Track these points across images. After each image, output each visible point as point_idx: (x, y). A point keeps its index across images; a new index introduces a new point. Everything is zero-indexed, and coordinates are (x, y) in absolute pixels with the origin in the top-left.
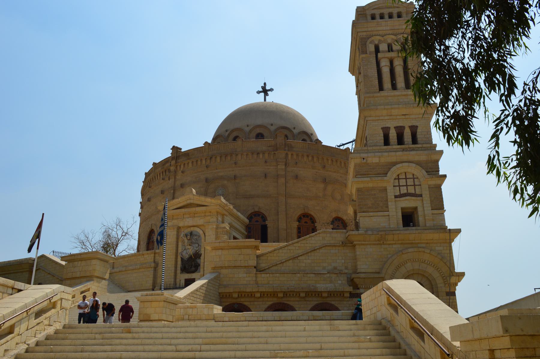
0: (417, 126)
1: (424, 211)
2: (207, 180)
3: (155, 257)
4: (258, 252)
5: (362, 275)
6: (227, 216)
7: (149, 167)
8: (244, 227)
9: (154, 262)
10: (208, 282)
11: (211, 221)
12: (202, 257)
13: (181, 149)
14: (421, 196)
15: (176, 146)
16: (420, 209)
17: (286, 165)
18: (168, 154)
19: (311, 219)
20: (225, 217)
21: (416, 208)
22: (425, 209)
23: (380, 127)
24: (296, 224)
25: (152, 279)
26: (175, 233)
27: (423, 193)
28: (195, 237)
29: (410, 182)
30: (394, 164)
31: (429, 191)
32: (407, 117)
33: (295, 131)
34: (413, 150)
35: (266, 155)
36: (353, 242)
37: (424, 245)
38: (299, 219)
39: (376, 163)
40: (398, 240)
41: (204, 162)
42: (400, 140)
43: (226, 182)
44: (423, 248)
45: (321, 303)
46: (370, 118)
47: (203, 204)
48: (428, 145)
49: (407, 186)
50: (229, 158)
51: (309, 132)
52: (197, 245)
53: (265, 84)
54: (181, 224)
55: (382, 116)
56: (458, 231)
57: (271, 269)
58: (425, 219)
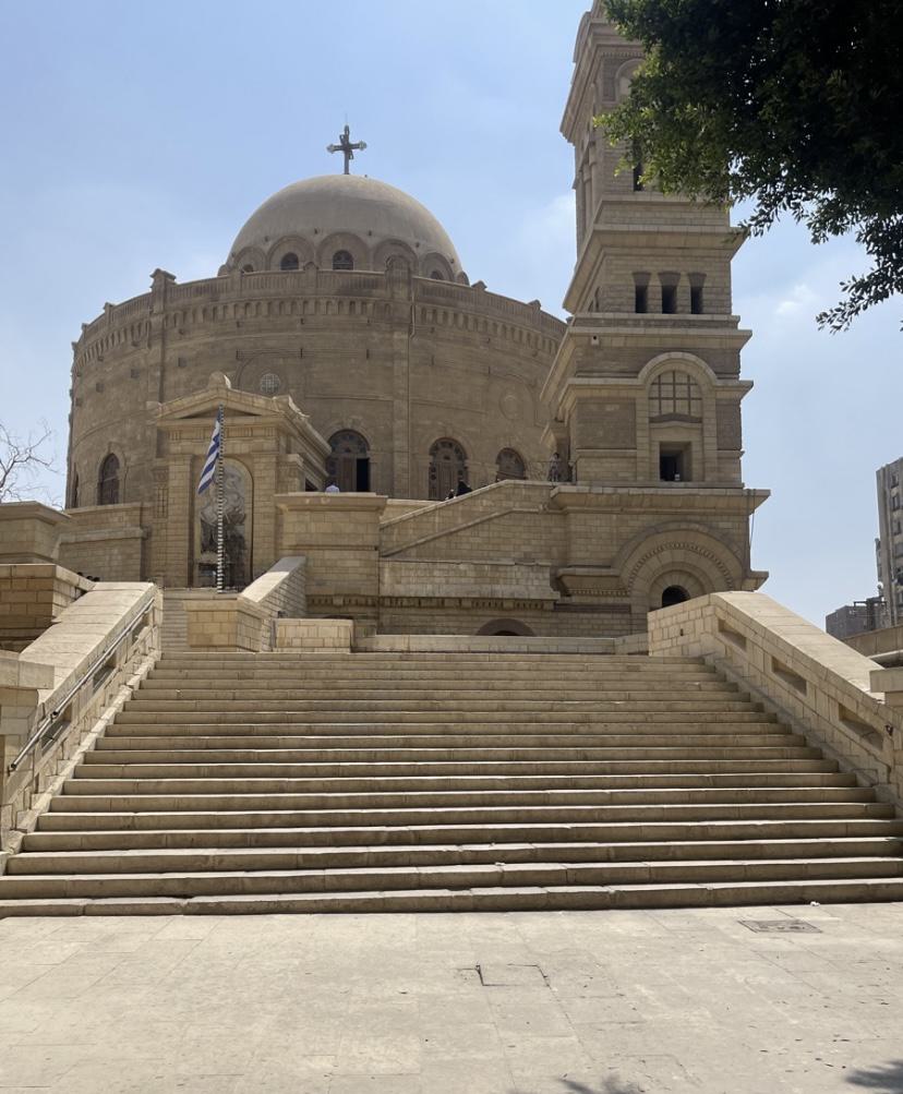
0: (705, 275)
1: (704, 448)
3: (141, 515)
4: (384, 520)
5: (580, 571)
6: (295, 438)
7: (94, 312)
10: (289, 578)
11: (240, 438)
12: (247, 522)
13: (174, 278)
14: (700, 420)
15: (163, 269)
16: (695, 448)
18: (144, 286)
19: (457, 451)
21: (688, 445)
22: (706, 447)
23: (630, 272)
24: (427, 460)
25: (139, 562)
26: (188, 468)
27: (706, 414)
28: (232, 480)
29: (681, 391)
30: (654, 352)
31: (717, 412)
32: (686, 252)
33: (420, 252)
34: (691, 324)
36: (566, 505)
37: (698, 518)
38: (434, 450)
39: (619, 348)
40: (651, 506)
41: (231, 311)
42: (668, 305)
44: (697, 522)
45: (498, 621)
46: (613, 250)
47: (248, 410)
48: (724, 318)
49: (674, 398)
51: (448, 256)
52: (236, 497)
53: (347, 129)
55: (637, 247)
56: (764, 495)
58: (704, 469)
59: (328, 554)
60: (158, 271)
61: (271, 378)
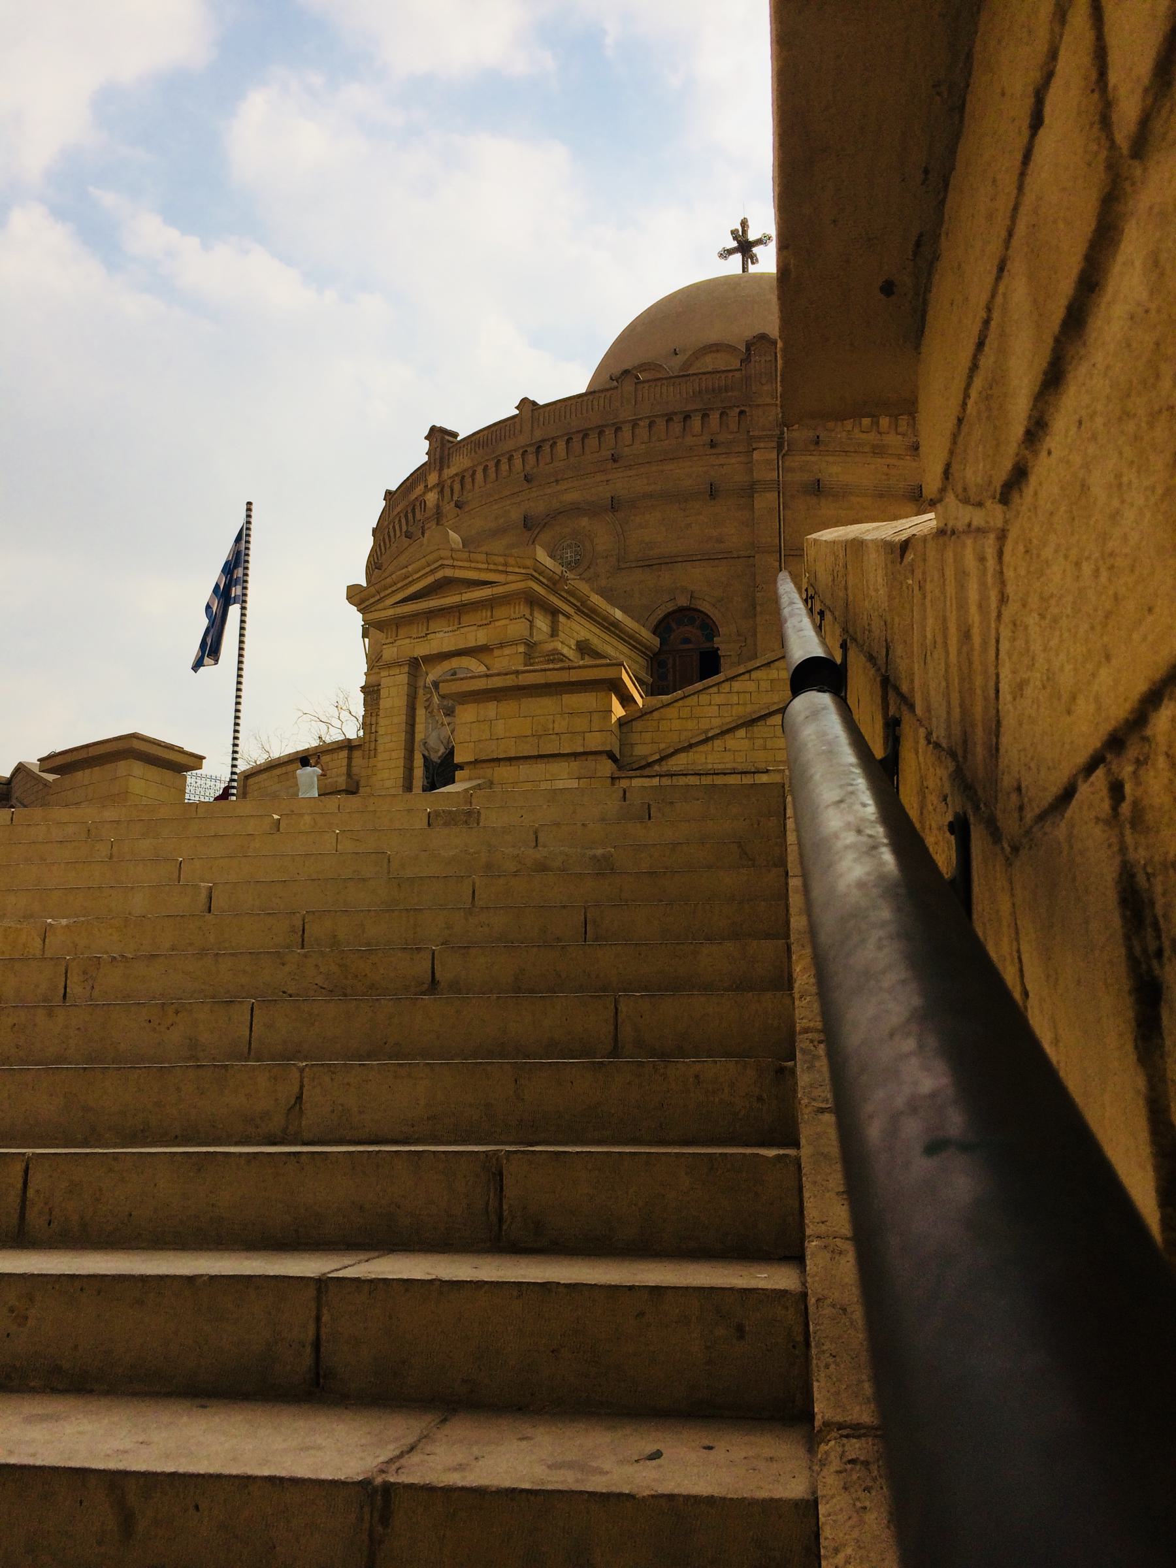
2: (528, 523)
6: (568, 617)
8: (644, 663)
9: (349, 774)
13: (455, 435)
17: (780, 447)
18: (418, 454)
20: (562, 618)
35: (715, 417)
41: (518, 461)
43: (584, 522)
50: (593, 441)
53: (744, 223)
54: (421, 650)
57: (672, 761)
59: (525, 770)
60: (433, 429)
61: (570, 546)
